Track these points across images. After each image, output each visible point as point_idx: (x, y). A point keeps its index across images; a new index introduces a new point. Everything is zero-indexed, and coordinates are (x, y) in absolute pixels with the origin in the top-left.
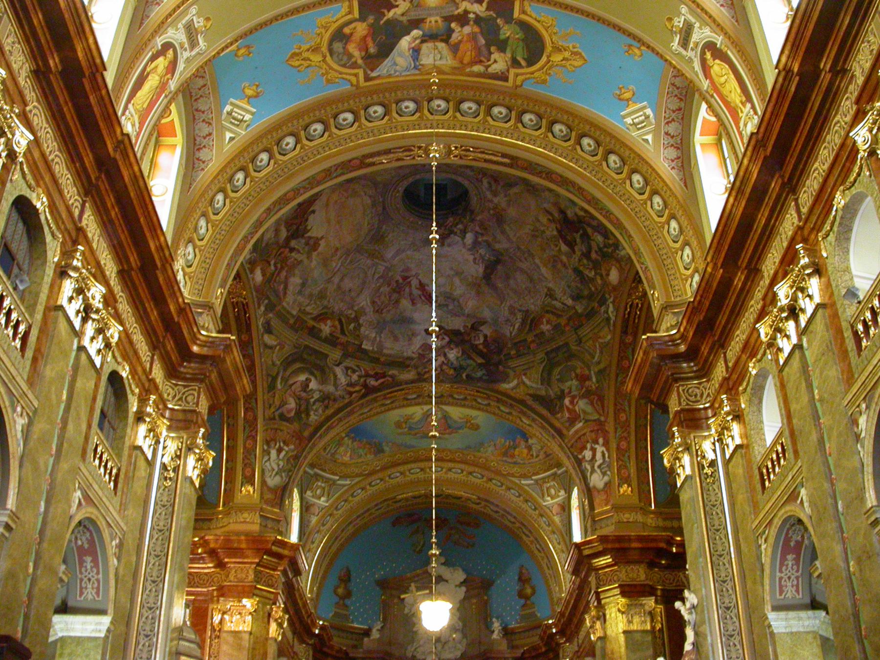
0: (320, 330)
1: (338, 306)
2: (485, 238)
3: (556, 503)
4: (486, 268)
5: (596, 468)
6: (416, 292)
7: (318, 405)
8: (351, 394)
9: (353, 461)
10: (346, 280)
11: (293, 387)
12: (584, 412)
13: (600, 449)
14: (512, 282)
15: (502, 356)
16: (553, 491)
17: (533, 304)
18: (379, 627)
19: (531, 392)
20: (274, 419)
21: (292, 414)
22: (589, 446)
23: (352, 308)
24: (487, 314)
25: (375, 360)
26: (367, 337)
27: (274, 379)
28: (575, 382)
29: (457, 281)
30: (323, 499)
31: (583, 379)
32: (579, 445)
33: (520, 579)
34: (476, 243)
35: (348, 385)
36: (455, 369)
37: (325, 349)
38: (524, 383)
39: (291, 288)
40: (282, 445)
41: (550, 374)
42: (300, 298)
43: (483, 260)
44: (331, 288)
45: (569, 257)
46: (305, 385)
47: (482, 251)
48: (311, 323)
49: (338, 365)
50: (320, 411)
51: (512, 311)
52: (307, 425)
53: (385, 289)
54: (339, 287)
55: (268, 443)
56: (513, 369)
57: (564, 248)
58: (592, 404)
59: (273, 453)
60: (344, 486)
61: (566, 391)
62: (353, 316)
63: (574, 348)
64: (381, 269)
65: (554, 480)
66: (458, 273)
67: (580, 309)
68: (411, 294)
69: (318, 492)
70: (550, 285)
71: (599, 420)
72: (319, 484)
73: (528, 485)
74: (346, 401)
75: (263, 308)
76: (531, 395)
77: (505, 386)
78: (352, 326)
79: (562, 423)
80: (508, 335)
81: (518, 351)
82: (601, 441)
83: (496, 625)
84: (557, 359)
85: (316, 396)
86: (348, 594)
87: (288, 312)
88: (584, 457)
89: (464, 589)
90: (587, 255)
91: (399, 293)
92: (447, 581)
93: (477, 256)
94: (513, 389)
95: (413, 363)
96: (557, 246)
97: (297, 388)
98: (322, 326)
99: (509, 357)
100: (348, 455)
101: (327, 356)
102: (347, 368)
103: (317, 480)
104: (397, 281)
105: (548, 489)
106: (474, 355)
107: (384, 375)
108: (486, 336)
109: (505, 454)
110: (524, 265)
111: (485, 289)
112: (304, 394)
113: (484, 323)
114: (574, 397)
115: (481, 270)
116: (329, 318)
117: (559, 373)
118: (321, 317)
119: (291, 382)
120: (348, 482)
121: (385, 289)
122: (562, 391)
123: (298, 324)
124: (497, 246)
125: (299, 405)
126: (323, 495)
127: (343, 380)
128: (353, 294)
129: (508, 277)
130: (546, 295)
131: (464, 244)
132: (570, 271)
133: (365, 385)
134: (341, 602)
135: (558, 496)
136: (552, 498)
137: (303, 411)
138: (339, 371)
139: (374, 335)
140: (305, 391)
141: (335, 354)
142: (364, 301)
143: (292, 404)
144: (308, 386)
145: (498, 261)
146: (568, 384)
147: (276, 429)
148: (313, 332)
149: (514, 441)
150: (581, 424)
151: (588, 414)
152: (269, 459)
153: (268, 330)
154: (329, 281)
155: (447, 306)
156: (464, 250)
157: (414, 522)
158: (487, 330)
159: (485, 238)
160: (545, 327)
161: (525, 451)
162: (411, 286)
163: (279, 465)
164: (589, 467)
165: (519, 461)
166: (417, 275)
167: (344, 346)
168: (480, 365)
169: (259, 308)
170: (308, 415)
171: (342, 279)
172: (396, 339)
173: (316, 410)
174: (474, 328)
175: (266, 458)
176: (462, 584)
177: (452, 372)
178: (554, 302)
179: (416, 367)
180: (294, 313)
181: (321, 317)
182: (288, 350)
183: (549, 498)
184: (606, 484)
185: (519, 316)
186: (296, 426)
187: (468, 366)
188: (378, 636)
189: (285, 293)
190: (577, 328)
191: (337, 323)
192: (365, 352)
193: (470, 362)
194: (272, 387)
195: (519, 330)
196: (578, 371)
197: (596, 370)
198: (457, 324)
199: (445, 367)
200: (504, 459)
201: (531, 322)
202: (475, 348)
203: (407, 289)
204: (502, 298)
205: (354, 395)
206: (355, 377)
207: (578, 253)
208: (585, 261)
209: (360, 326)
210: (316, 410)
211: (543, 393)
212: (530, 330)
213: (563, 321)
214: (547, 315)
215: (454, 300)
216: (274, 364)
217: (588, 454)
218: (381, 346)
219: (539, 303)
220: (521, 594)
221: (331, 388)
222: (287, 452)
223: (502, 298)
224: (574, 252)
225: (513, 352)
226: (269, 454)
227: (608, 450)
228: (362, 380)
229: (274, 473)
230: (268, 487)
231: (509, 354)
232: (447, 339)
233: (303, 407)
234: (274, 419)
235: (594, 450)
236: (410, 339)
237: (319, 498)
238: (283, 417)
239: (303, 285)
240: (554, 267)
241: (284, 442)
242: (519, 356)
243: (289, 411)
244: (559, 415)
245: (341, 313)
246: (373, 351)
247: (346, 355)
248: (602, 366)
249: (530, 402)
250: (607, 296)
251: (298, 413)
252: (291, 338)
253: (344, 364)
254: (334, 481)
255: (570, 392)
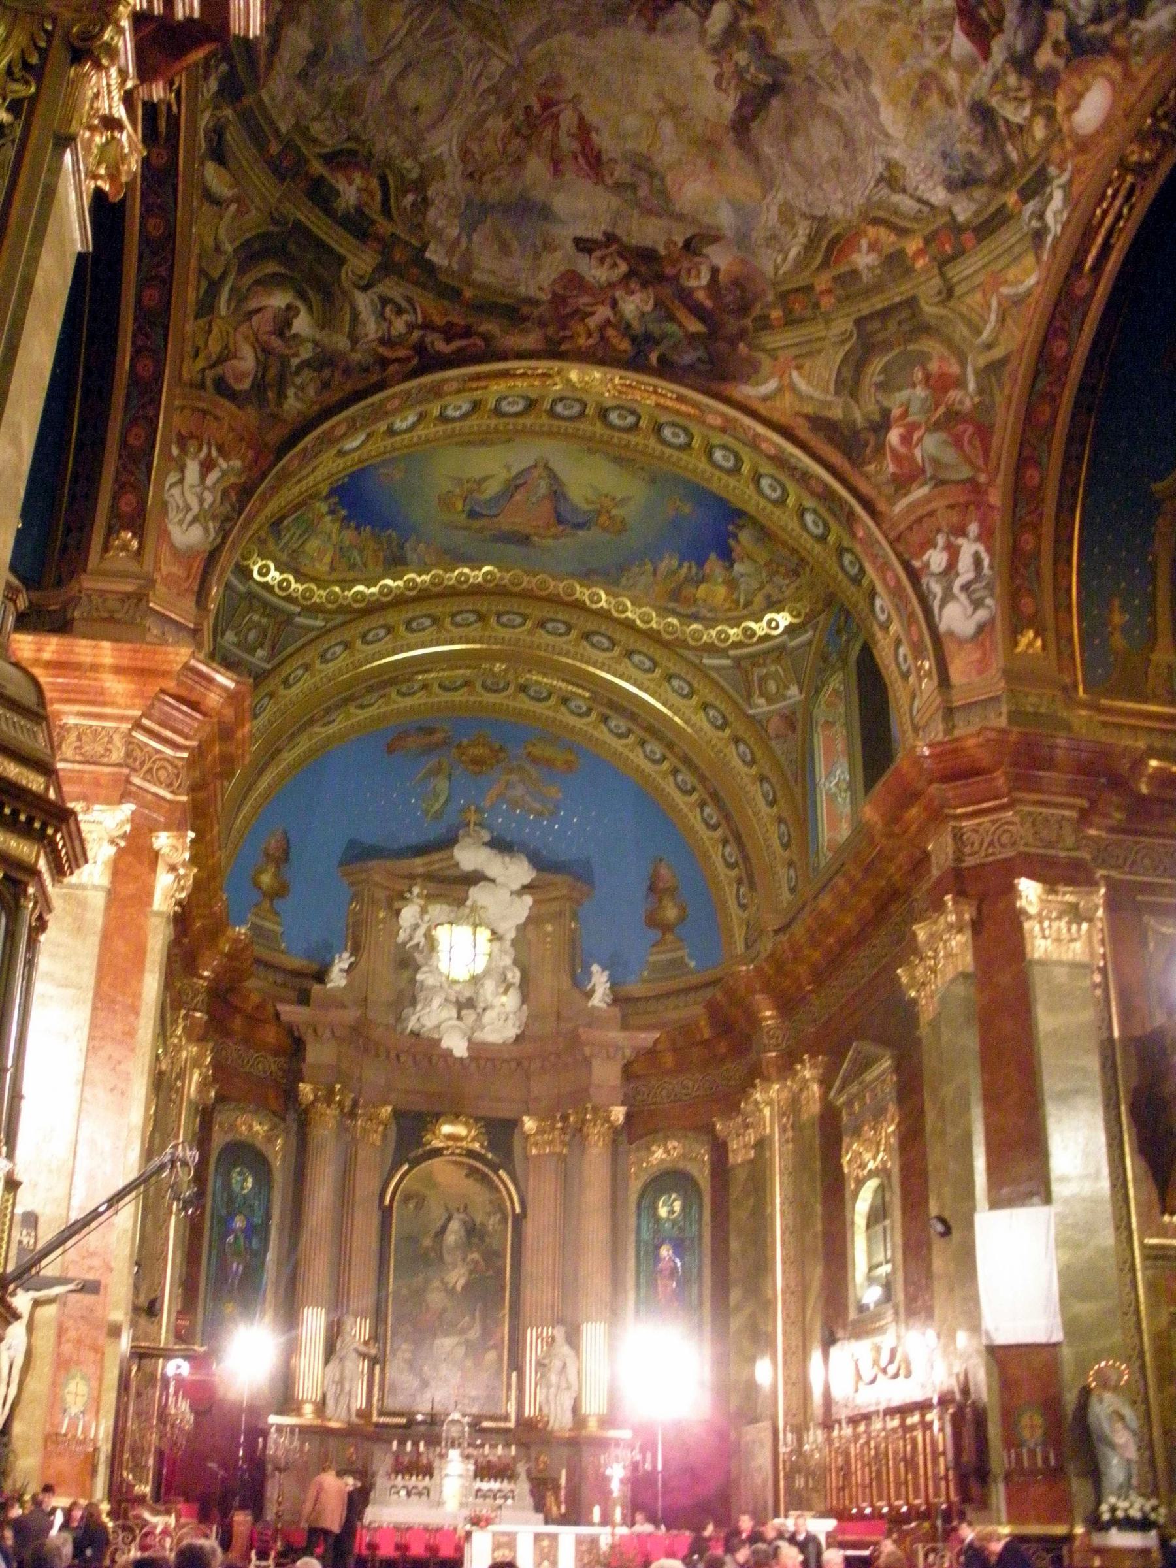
0: (337, 194)
1: (388, 144)
2: (756, 21)
3: (778, 712)
4: (743, 102)
5: (956, 588)
6: (568, 145)
7: (307, 374)
8: (384, 363)
9: (335, 576)
10: (413, 80)
11: (255, 320)
12: (935, 462)
13: (968, 549)
14: (798, 144)
15: (748, 322)
16: (772, 686)
17: (841, 201)
18: (345, 965)
19: (809, 409)
20: (202, 386)
21: (246, 385)
22: (941, 540)
23: (414, 153)
24: (725, 219)
25: (454, 294)
26: (438, 234)
27: (214, 288)
28: (920, 392)
29: (667, 127)
30: (260, 653)
31: (941, 384)
32: (915, 538)
33: (652, 888)
34: (731, 32)
35: (382, 341)
36: (634, 340)
37: (339, 241)
38: (793, 388)
39: (285, 54)
40: (214, 453)
41: (859, 367)
42: (301, 96)
43: (741, 79)
44: (378, 88)
45: (967, 69)
46: (283, 322)
47: (742, 57)
48: (317, 167)
49: (364, 289)
50: (311, 391)
51: (787, 215)
52: (275, 418)
53: (497, 124)
54: (393, 95)
55: (182, 442)
56: (772, 354)
57: (961, 44)
58: (957, 443)
59: (192, 469)
60: (309, 629)
61: (896, 412)
62: (414, 175)
63: (929, 309)
64: (497, 68)
65: (778, 660)
66: (674, 110)
67: (963, 211)
68: (554, 146)
69: (252, 636)
70: (896, 154)
71: (972, 481)
72: (256, 618)
73: (717, 669)
74: (374, 378)
75: (213, 84)
76: (807, 417)
77: (747, 391)
78: (410, 198)
79: (877, 487)
80: (770, 271)
81: (788, 312)
82: (973, 529)
83: (600, 980)
84: (881, 336)
85: (306, 352)
86: (281, 891)
87: (272, 123)
88: (927, 565)
89: (528, 900)
90: (1022, 63)
91: (526, 138)
92: (493, 881)
93: (728, 68)
94: (765, 399)
95: (537, 312)
96: (939, 40)
97: (263, 324)
98: (342, 185)
99: (764, 324)
100: (327, 559)
101: (341, 261)
102: (384, 301)
103: (251, 609)
104: (528, 109)
105: (762, 680)
106: (681, 314)
107: (467, 332)
108: (715, 271)
109: (676, 595)
110: (839, 102)
111: (732, 155)
112: (276, 343)
113: (716, 239)
114: (911, 428)
115: (730, 106)
116: (357, 166)
117: (884, 370)
118: (340, 160)
119: (252, 305)
120: (319, 623)
121: (497, 124)
122: (886, 413)
123: (286, 166)
124: (782, 47)
125: (263, 367)
126: (261, 646)
127: (371, 328)
128: (423, 119)
129: (790, 129)
130: (881, 179)
131: (703, 32)
132: (960, 114)
133: (420, 349)
134: (266, 904)
135: (784, 698)
136: (770, 700)
137: (268, 385)
138: (363, 302)
139: (454, 232)
140: (281, 334)
141: (360, 261)
142: (443, 144)
143: (247, 361)
144: (289, 325)
145: (774, 89)
146: (902, 396)
147: (205, 413)
148: (320, 194)
149: (701, 564)
150: (925, 490)
151: (946, 466)
152: (181, 481)
153: (219, 155)
154: (373, 68)
155: (634, 187)
156: (699, 51)
157: (431, 749)
158: (721, 257)
159: (756, 21)
160: (864, 260)
161: (721, 591)
162: (557, 126)
163: (201, 501)
164: (937, 588)
165: (704, 612)
166: (576, 100)
167: (386, 245)
168: (692, 337)
169: (206, 77)
170: (281, 396)
171: (402, 75)
172: (505, 249)
173: (302, 388)
174: (691, 247)
175: (173, 478)
176: (527, 888)
177: (625, 345)
178: (897, 198)
179: (542, 323)
180: (284, 129)
181: (340, 160)
182: (254, 222)
183: (762, 701)
184: (981, 628)
185: (803, 229)
186: (250, 416)
187: (664, 336)
188: (343, 983)
189: (270, 65)
190: (943, 263)
191: (375, 183)
192: (430, 269)
193: (671, 327)
194: (206, 307)
195: (801, 264)
196: (933, 367)
197: (982, 361)
198: (650, 233)
199: (611, 332)
200: (672, 605)
201: (829, 244)
202: (685, 296)
203: (548, 133)
204: (768, 184)
205: (393, 368)
206: (399, 326)
207: (998, 54)
208: (1012, 80)
209: (426, 202)
210: (302, 388)
211: (837, 413)
212: (825, 264)
213: (912, 245)
214: (872, 231)
215: (652, 175)
216: (218, 248)
217: (937, 559)
218: (468, 263)
219: (858, 200)
220: (653, 921)
221: (341, 342)
222: (224, 474)
223: (768, 184)
224: (986, 53)
225: (776, 314)
226: (182, 469)
227: (989, 550)
228: (416, 334)
229: (189, 517)
230: (172, 545)
231: (767, 317)
232: (623, 267)
233: (272, 374)
234: (202, 386)
235: (953, 552)
236: (537, 256)
237: (252, 651)
238: (222, 387)
239: (314, 57)
240: (917, 103)
241: (221, 449)
242: (790, 321)
243: (239, 377)
244: (871, 468)
245: (388, 163)
246: (448, 270)
247: (385, 268)
248: (998, 353)
249: (804, 432)
250: (1052, 170)
251: (259, 385)
252: (265, 189)
253: (380, 289)
254: (290, 616)
255: (905, 414)
